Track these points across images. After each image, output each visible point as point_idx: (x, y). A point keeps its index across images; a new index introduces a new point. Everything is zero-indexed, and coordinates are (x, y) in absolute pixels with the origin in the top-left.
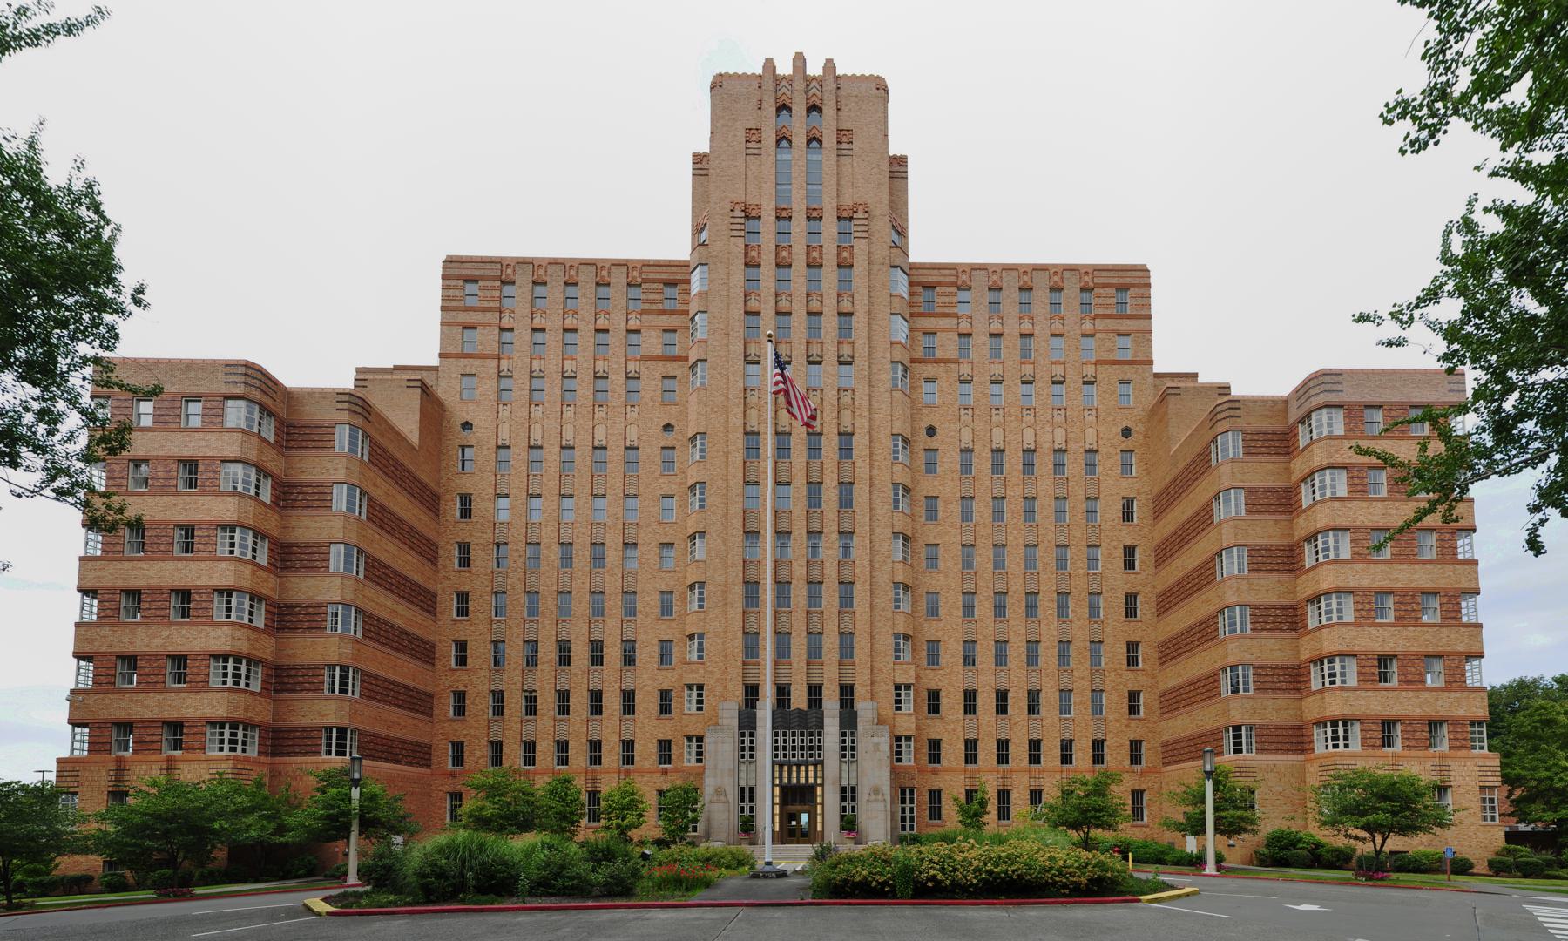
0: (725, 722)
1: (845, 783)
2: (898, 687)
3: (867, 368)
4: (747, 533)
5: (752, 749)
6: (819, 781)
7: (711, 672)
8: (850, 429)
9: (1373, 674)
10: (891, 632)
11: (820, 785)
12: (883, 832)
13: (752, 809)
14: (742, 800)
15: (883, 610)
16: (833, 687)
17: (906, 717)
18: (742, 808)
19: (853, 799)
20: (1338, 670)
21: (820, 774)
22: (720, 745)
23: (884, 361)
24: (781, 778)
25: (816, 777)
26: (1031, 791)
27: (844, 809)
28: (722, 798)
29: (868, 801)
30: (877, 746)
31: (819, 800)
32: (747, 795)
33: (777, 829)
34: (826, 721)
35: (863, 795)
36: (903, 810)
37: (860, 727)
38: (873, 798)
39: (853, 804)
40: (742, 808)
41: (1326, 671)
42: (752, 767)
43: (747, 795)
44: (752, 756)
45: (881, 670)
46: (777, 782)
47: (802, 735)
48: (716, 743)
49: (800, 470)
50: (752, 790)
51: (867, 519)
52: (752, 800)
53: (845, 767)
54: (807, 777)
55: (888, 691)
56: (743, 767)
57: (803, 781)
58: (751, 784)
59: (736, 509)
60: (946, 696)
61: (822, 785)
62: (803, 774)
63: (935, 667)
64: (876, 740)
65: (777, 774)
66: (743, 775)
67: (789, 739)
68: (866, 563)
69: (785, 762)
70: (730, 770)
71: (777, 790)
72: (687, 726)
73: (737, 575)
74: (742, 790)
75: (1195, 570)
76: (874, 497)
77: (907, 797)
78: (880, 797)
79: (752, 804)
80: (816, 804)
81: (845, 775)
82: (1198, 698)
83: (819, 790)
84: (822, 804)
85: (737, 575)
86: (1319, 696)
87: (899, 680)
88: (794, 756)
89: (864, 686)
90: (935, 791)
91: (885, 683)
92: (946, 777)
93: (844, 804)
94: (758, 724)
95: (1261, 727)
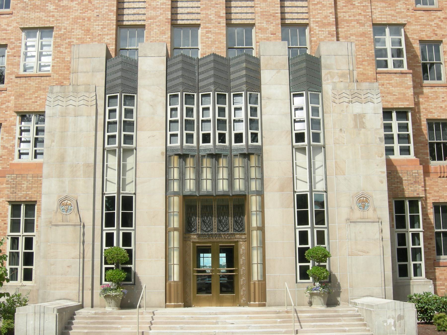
0: (82, 79)
5: (129, 125)
6: (254, 186)
7: (65, 8)
12: (379, 279)
13: (127, 239)
14: (110, 221)
16: (271, 28)
17: (396, 79)
18: (110, 237)
21: (253, 173)
22: (71, 119)
24: (182, 180)
25: (247, 179)
27: (303, 237)
28: (73, 217)
29: (350, 221)
31: (255, 222)
32: (118, 212)
33: (176, 276)
36: (402, 239)
38: (358, 214)
39: (320, 227)
40: (110, 237)
43: (118, 212)
44: (129, 139)
46: (175, 187)
48: (64, 115)
54: (231, 180)
55: (363, 34)
56: (113, 161)
57: (223, 186)
58: (129, 190)
61: (260, 193)
62: (223, 173)
63: (428, 7)
64: (357, 108)
65: (175, 174)
66: (112, 175)
69: (191, 149)
70: (88, 166)
71: (176, 201)
72: (21, 95)
74: (110, 201)
77: (408, 215)
78: (370, 213)
79: (127, 229)
83: (254, 202)
84: (262, 229)
87: (380, 18)
88: (206, 138)
89: (324, 25)
91: (358, 21)
93: (303, 228)
94: (141, 82)
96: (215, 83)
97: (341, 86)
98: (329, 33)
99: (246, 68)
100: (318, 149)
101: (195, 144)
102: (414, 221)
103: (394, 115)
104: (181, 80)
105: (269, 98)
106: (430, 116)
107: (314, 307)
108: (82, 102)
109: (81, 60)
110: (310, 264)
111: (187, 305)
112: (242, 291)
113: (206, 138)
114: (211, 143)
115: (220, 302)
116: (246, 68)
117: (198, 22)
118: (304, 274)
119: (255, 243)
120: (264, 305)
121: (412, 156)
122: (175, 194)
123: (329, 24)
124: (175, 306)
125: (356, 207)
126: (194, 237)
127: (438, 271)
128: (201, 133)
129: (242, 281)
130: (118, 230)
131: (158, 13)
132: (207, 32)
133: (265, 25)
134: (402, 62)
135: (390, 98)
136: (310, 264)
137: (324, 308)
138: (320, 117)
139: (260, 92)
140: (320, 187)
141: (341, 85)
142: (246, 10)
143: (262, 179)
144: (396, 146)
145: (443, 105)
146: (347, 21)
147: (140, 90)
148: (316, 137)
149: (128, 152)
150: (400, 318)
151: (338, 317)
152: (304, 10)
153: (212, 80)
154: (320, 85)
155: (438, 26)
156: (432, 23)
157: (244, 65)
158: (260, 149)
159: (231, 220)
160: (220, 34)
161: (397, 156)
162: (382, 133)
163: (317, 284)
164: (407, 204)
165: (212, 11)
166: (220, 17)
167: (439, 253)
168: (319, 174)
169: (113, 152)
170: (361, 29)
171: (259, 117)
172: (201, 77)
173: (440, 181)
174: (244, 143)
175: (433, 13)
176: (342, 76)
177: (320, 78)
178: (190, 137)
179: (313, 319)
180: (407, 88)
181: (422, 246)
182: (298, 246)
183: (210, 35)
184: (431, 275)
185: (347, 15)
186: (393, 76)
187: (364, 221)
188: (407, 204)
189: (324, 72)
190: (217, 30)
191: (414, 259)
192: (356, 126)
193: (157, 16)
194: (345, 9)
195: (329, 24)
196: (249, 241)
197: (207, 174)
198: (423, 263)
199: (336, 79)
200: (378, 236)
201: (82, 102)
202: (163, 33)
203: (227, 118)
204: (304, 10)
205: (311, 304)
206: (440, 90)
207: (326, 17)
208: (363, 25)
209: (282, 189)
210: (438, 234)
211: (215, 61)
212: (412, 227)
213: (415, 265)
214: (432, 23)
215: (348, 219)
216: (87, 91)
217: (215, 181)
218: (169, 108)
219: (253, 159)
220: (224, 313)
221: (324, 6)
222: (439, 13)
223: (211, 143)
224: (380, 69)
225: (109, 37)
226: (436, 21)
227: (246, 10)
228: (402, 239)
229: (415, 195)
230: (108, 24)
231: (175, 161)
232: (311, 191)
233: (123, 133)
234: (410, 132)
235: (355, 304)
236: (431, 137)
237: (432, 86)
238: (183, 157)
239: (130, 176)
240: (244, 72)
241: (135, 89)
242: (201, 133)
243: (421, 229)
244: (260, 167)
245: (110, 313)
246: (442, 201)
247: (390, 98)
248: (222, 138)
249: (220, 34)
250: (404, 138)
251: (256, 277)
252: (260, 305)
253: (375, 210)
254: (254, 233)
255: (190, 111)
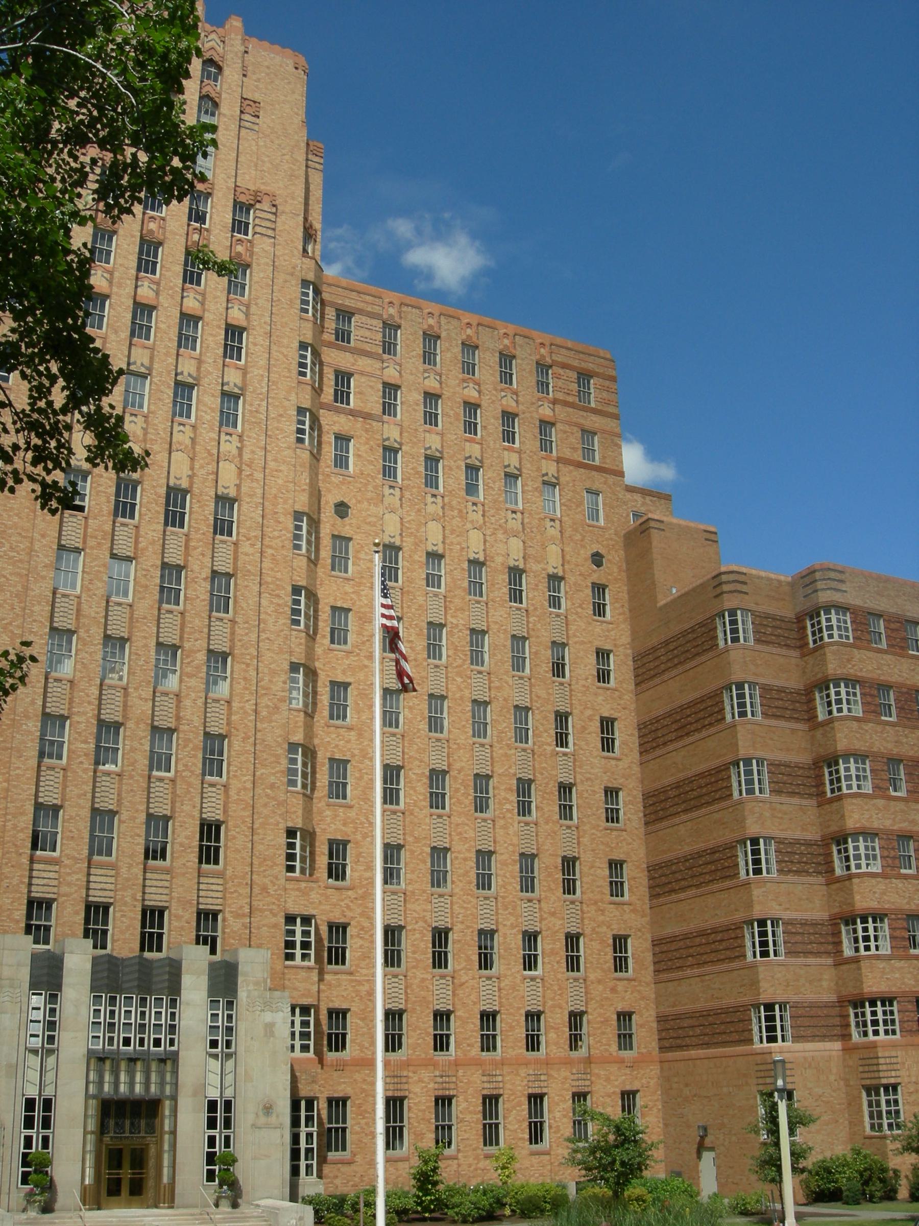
1: (213, 1093)
2: (290, 919)
3: (263, 409)
4: (53, 629)
5: (51, 1025)
6: (168, 1090)
8: (232, 493)
9: (903, 938)
10: (283, 826)
11: (167, 1098)
14: (29, 1123)
15: (272, 786)
17: (303, 974)
18: (28, 1141)
19: (227, 1124)
20: (871, 933)
21: (168, 1078)
23: (286, 403)
24: (100, 1083)
25: (162, 1084)
26: (485, 1098)
27: (212, 1141)
30: (269, 1029)
32: (38, 1114)
34: (187, 980)
35: (244, 1116)
37: (242, 994)
38: (262, 1120)
39: (226, 1132)
41: (860, 934)
42: (51, 1060)
43: (38, 1114)
44: (51, 1039)
45: (264, 889)
47: (143, 1001)
49: (153, 542)
50: (48, 1104)
51: (254, 636)
52: (46, 1123)
53: (215, 1065)
54: (147, 1084)
55: (275, 926)
58: (48, 1092)
59: (42, 589)
60: (358, 936)
61: (174, 1098)
62: (138, 1077)
64: (268, 1017)
66: (34, 1076)
67: (121, 1009)
68: (249, 707)
69: (111, 1052)
71: (93, 1103)
73: (33, 702)
74: (30, 1104)
75: (701, 775)
76: (264, 602)
77: (303, 1114)
78: (273, 1119)
80: (162, 1133)
81: (214, 1079)
82: (713, 957)
84: (174, 1133)
85: (33, 702)
86: (854, 966)
87: (294, 909)
89: (237, 916)
90: (337, 1100)
91: (271, 911)
92: (357, 1076)
93: (212, 1132)
95: (795, 1006)
96: (138, 986)
97: (256, 993)
98: (243, 925)
99: (169, 973)
100: (229, 1056)
101: (115, 1047)
102: (309, 1119)
103: (297, 1011)
104: (106, 981)
105: (188, 1004)
106: (331, 1005)
107: (221, 1208)
108: (6, 999)
109: (6, 952)
110: (217, 1168)
111: (99, 1209)
112: (150, 1192)
113: (127, 1042)
114: (132, 1047)
115: (129, 1205)
116: (169, 973)
117: (111, 900)
118: (211, 1176)
119: (166, 1147)
120: (172, 1207)
121: (311, 1054)
122: (94, 1097)
123: (244, 915)
124: (90, 1209)
125: (261, 1113)
126: (107, 1139)
127: (326, 1169)
128: (122, 1036)
129: (151, 1183)
130: (38, 1133)
131: (73, 890)
132: (123, 916)
133: (180, 912)
134: (309, 955)
135: (295, 994)
136: (217, 1168)
137: (230, 1210)
138: (234, 1024)
139: (180, 996)
140: (228, 1093)
141: (256, 993)
142: (160, 891)
143: (176, 1084)
144: (298, 1043)
145: (345, 994)
146: (261, 911)
147: (64, 988)
148: (228, 1044)
149: (50, 1052)
150: (301, 1219)
151: (245, 1219)
152: (219, 895)
153: (136, 983)
154: (236, 991)
155: (348, 907)
156: (342, 904)
157: (167, 969)
158: (176, 1053)
159: (143, 1123)
160: (135, 919)
161: (298, 1053)
162: (289, 1042)
163: (225, 1187)
164: (303, 1103)
165: (129, 892)
166: (136, 900)
167: (329, 1150)
168: (229, 1079)
169: (35, 1052)
170: (274, 920)
171: (176, 1022)
172: (126, 978)
173: (336, 1074)
174: (162, 1048)
175: (344, 892)
176: (257, 983)
177: (236, 984)
178: (111, 1039)
179: (225, 1220)
180: (313, 984)
181: (315, 1145)
182: (206, 1149)
183: (124, 919)
184: (320, 1176)
185: (261, 903)
186: (300, 971)
187: (268, 1126)
188: (303, 1103)
189: (240, 979)
190: (132, 915)
191: (306, 1159)
192: (266, 1035)
193: (71, 894)
194: (260, 897)
195: (244, 915)
196: (160, 1143)
197: (123, 1077)
198: (315, 1163)
199: (251, 987)
200: (279, 1141)
201: (6, 999)
202: (77, 913)
203: (147, 1021)
204: (219, 895)
205: (217, 1205)
206: (344, 977)
207: (241, 907)
208: (275, 915)
209: (195, 1094)
210: (330, 1129)
211: (140, 964)
212: (307, 1126)
213: (307, 1166)
214: (342, 904)
215: (253, 1125)
216: (11, 986)
217: (132, 1084)
218: (92, 1008)
219: (169, 1063)
220: (145, 1216)
221: (240, 895)
222: (350, 893)
223: (132, 1047)
224: (287, 963)
225: (19, 913)
226: (346, 901)
227: (160, 891)
228: (295, 1139)
229: (312, 1094)
230: (19, 898)
231: (93, 1061)
232: (221, 1097)
233: (47, 1033)
234: (312, 1029)
235: (258, 1206)
236: (330, 1028)
237: (336, 973)
238: (101, 1060)
239: (50, 1077)
240: (166, 977)
241: (59, 987)
242: (122, 1036)
243: (315, 1129)
244: (175, 1072)
245: (35, 1218)
246: (336, 1095)
247: (295, 994)
248: (142, 1041)
249: (135, 919)
250: (305, 1035)
251: (165, 1180)
252: (170, 1207)
253: (277, 1116)
254: (167, 1137)
255: (112, 1013)
